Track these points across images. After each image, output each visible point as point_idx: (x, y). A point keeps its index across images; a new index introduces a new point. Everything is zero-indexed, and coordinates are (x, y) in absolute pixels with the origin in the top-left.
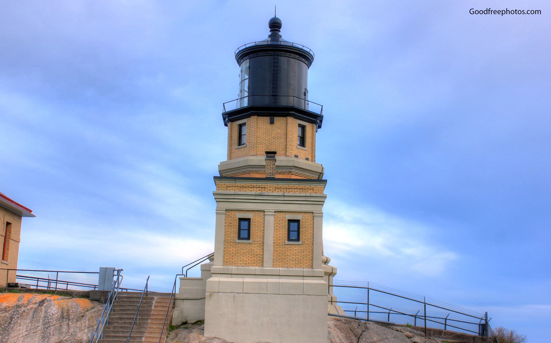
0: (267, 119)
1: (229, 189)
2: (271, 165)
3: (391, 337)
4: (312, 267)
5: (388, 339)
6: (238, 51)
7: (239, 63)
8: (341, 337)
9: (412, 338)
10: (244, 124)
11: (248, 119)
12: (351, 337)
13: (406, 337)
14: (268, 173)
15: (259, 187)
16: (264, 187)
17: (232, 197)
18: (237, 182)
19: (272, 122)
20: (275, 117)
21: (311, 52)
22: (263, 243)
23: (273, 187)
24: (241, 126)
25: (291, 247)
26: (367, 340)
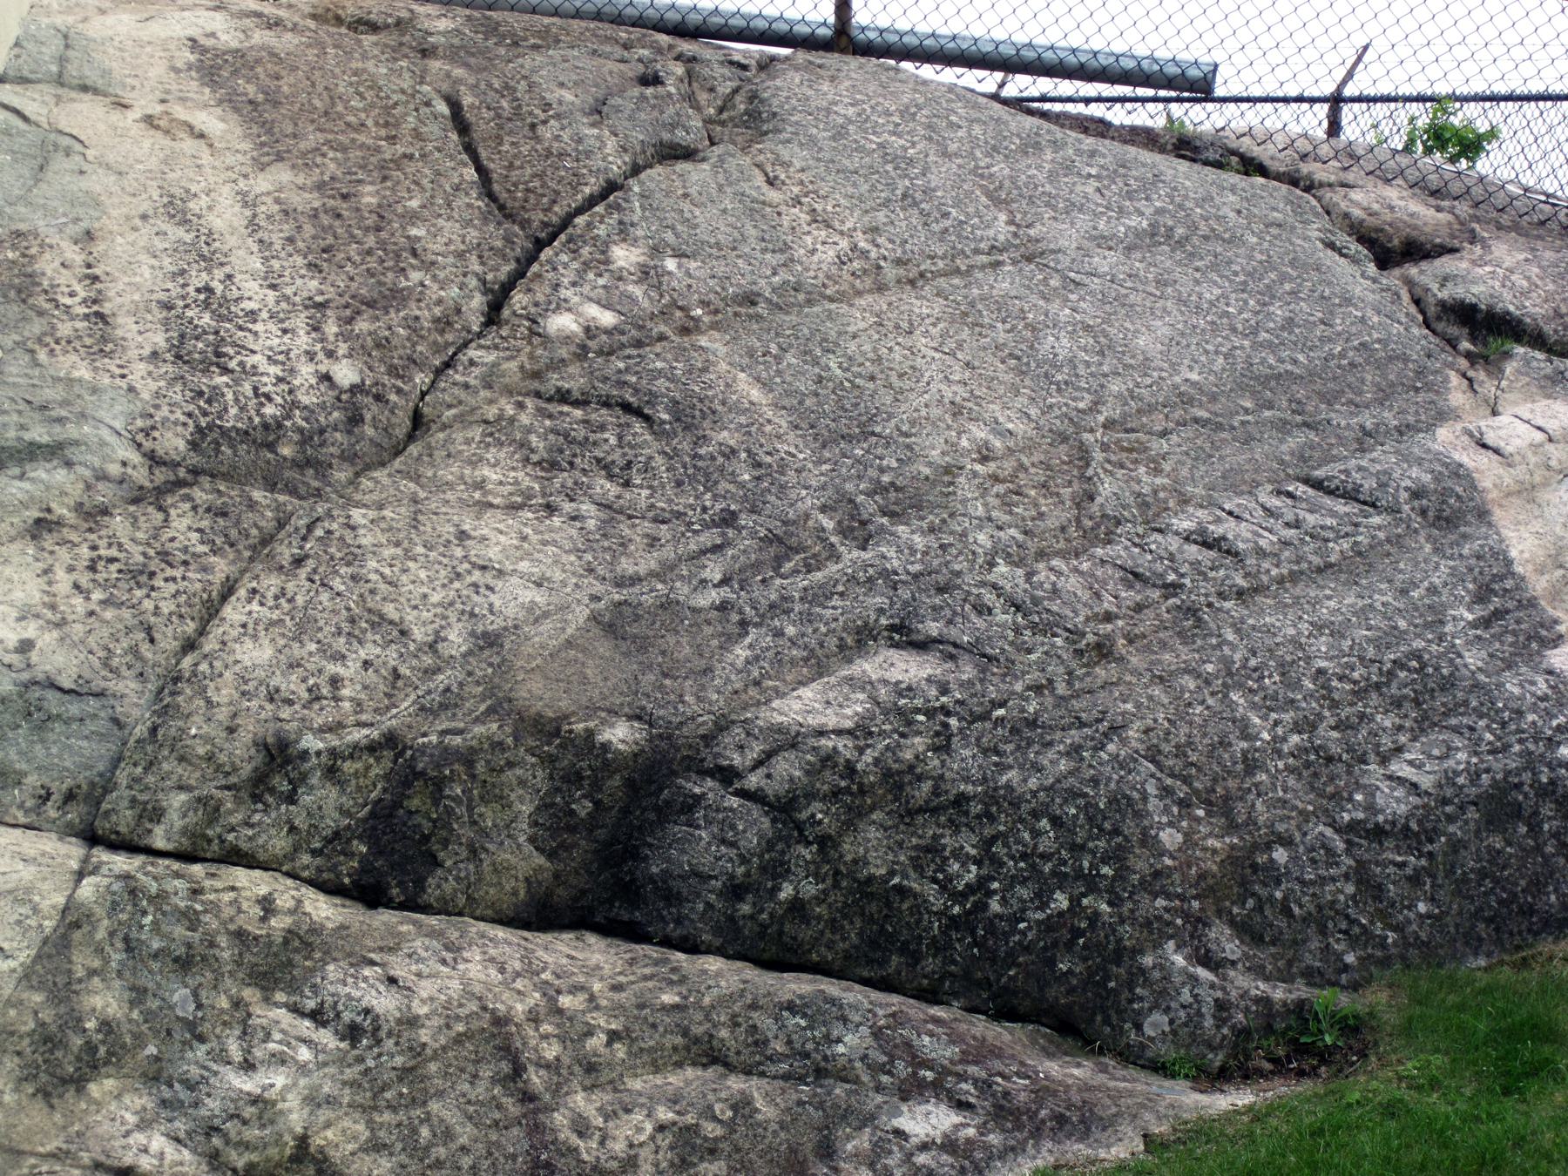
3: (1103, 242)
5: (1032, 255)
8: (225, 216)
9: (1445, 264)
12: (413, 217)
13: (1342, 238)
26: (671, 264)
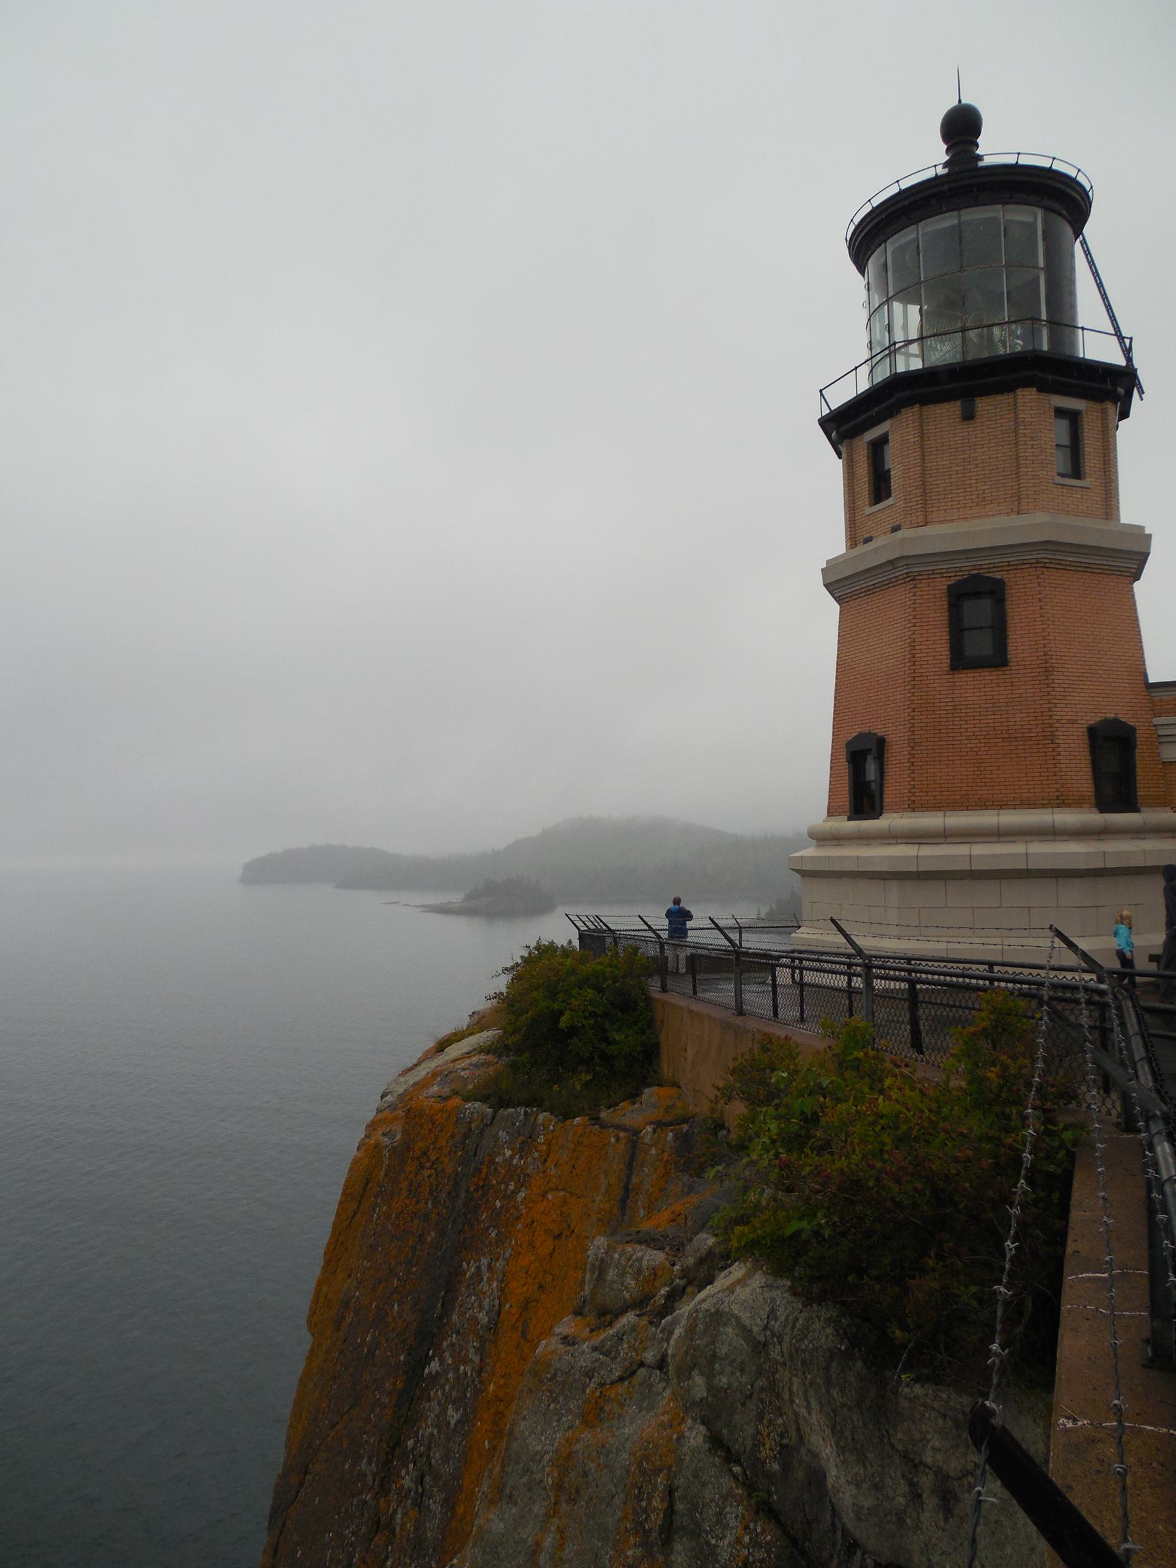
0: (953, 409)
6: (852, 228)
7: (862, 269)
10: (884, 440)
19: (968, 416)
20: (977, 400)
21: (1081, 179)
24: (878, 448)
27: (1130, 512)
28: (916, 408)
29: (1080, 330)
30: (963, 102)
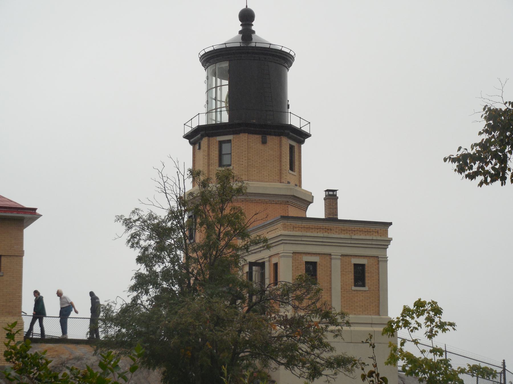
0: (257, 138)
1: (296, 230)
2: (333, 204)
4: (379, 314)
11: (235, 136)
14: (331, 213)
15: (325, 229)
16: (330, 228)
17: (300, 239)
18: (303, 222)
19: (264, 142)
20: (267, 136)
22: (331, 288)
23: (339, 229)
25: (358, 293)
27: (305, 186)
28: (246, 135)
29: (289, 114)
30: (248, 7)
